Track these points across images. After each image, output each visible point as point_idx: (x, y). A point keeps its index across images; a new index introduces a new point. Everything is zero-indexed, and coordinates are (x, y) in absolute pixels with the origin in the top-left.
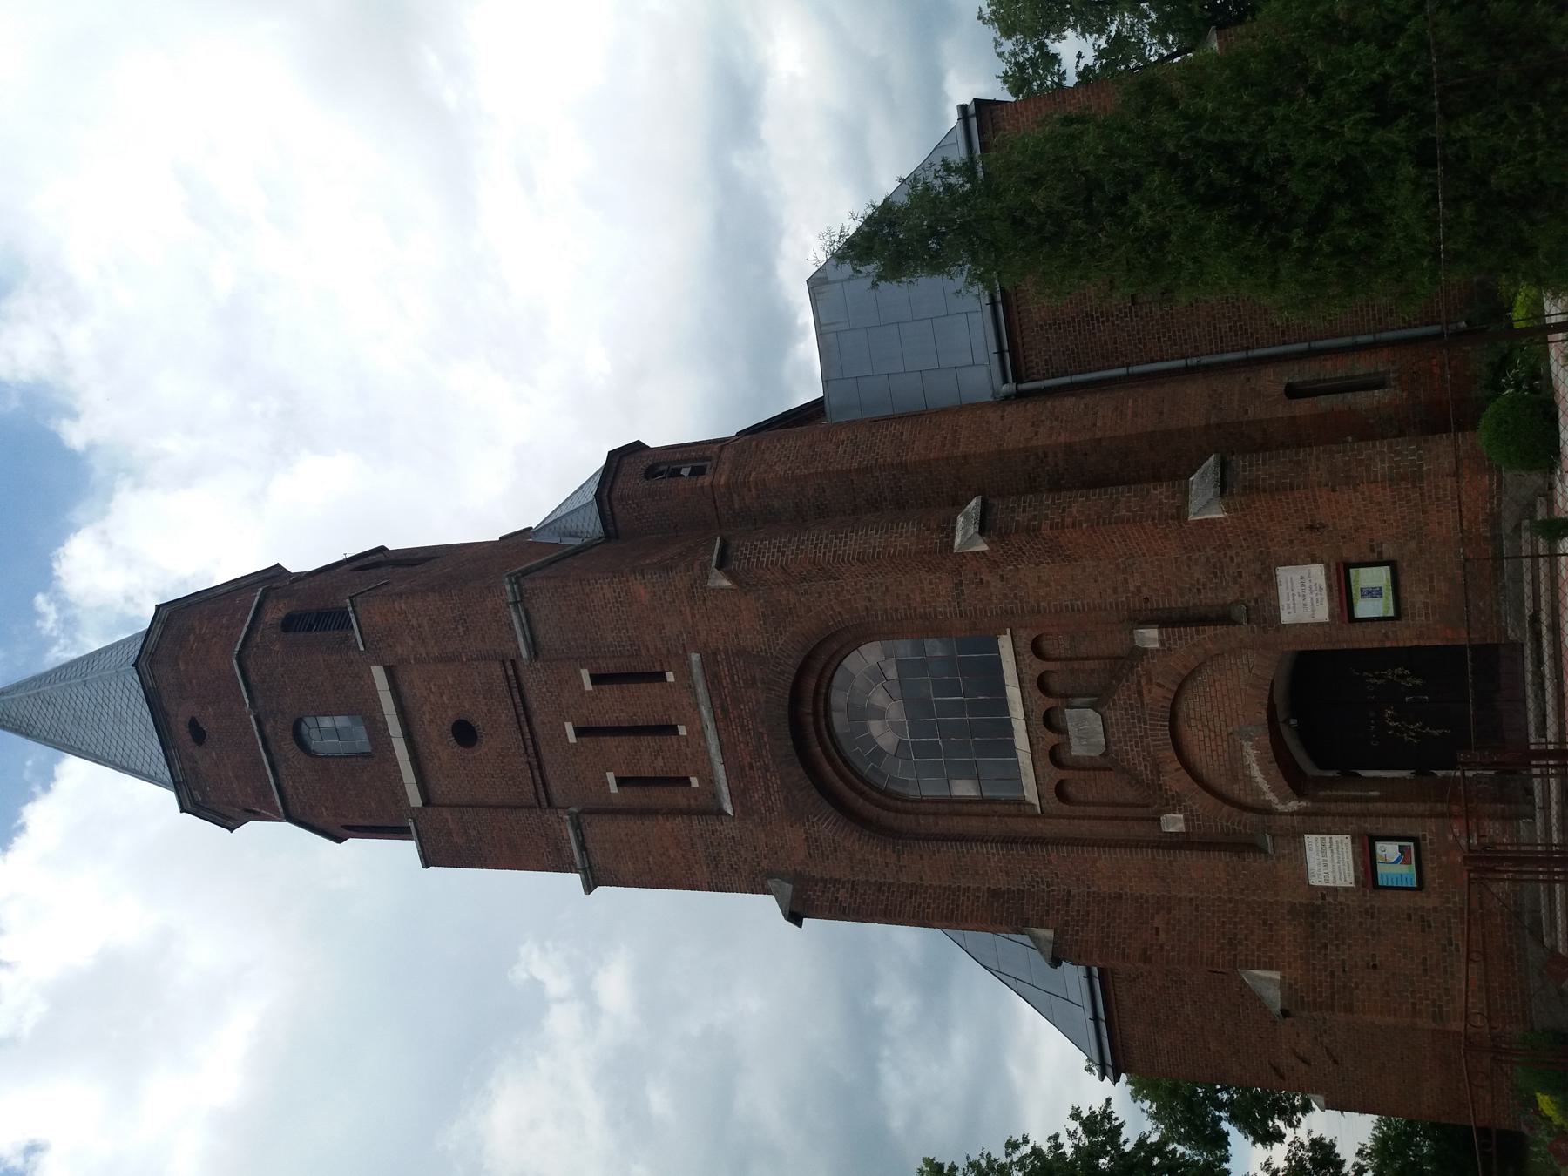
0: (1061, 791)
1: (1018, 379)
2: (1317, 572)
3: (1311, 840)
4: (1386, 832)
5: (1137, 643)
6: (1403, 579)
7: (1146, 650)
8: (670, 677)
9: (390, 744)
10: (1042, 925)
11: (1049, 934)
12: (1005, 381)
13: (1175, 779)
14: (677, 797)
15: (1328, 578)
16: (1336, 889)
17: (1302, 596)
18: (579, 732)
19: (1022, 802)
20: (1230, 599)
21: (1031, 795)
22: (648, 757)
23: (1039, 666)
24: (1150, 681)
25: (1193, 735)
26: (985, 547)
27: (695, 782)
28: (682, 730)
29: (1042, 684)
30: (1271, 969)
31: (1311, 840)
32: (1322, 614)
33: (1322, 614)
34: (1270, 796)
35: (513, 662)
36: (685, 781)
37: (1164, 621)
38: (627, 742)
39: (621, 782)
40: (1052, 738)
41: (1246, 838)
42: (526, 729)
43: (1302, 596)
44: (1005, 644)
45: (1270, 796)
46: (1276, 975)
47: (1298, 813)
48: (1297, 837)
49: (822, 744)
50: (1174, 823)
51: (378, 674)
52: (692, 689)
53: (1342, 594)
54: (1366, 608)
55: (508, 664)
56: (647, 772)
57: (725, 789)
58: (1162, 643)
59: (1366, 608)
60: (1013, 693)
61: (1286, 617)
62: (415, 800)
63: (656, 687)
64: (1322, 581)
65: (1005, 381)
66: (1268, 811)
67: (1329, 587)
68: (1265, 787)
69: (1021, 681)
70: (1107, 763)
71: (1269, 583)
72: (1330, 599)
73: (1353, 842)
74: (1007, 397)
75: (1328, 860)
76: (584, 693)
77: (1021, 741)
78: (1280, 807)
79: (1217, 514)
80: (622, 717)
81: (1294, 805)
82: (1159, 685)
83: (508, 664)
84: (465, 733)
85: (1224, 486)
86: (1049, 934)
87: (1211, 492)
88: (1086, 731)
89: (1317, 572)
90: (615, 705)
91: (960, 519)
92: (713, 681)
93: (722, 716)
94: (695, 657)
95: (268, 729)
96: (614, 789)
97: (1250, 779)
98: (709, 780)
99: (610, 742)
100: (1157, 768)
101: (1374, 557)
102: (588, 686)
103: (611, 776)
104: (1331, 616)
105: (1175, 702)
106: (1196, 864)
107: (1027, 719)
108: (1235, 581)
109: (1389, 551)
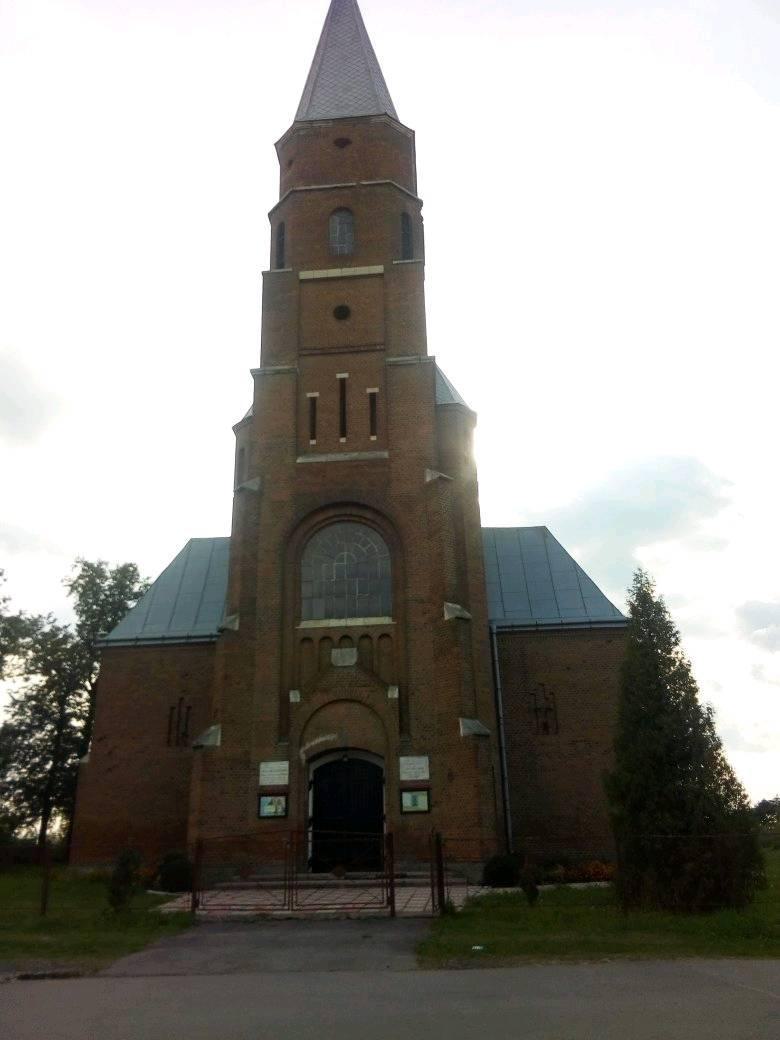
0: (307, 640)
1: (498, 634)
2: (425, 776)
3: (285, 765)
4: (290, 801)
5: (391, 688)
6: (420, 816)
7: (387, 690)
8: (373, 438)
9: (335, 267)
10: (240, 624)
11: (237, 628)
12: (498, 627)
13: (319, 699)
14: (306, 431)
15: (422, 781)
16: (258, 775)
17: (413, 768)
18: (343, 381)
19: (298, 619)
20: (413, 734)
21: (305, 625)
22: (328, 419)
23: (375, 635)
24: (372, 691)
25: (342, 709)
26: (447, 617)
27: (313, 442)
28: (343, 440)
29: (366, 636)
30: (222, 741)
31: (285, 765)
32: (404, 777)
33: (404, 777)
34: (308, 746)
35: (384, 350)
36: (313, 438)
37: (403, 700)
38: (336, 407)
39: (313, 400)
40: (336, 639)
41: (285, 733)
42: (346, 350)
43: (413, 768)
44: (386, 620)
45: (308, 746)
46: (219, 744)
47: (299, 759)
48: (287, 758)
49: (335, 516)
50: (294, 697)
51: (379, 269)
52: (367, 449)
53: (415, 787)
54: (407, 798)
55: (382, 347)
56: (319, 416)
57: (311, 460)
58: (391, 699)
59: (407, 798)
60: (359, 622)
61: (402, 760)
62: (304, 275)
63: (367, 428)
64: (421, 778)
65: (498, 627)
66: (301, 744)
67: (418, 781)
68: (313, 743)
69: (368, 626)
70: (325, 668)
71: (420, 752)
72: (411, 781)
73: (285, 786)
74: (490, 628)
75: (275, 773)
76: (366, 387)
77: (334, 623)
78: (302, 751)
79: (462, 732)
80: (351, 406)
81: (303, 757)
82: (368, 696)
83: (382, 347)
84: (342, 313)
85: (478, 736)
86: (237, 628)
87: (476, 730)
88: (345, 658)
89: (425, 776)
90: (357, 405)
91: (458, 607)
92: (373, 463)
93: (355, 465)
94: (386, 454)
95: (346, 192)
96: (309, 395)
97: (317, 736)
98: (315, 451)
99: (336, 397)
100: (326, 691)
101: (432, 803)
102: (369, 390)
103: (316, 394)
104: (405, 781)
105: (360, 702)
106: (272, 706)
107: (346, 627)
108: (422, 737)
109: (435, 810)
